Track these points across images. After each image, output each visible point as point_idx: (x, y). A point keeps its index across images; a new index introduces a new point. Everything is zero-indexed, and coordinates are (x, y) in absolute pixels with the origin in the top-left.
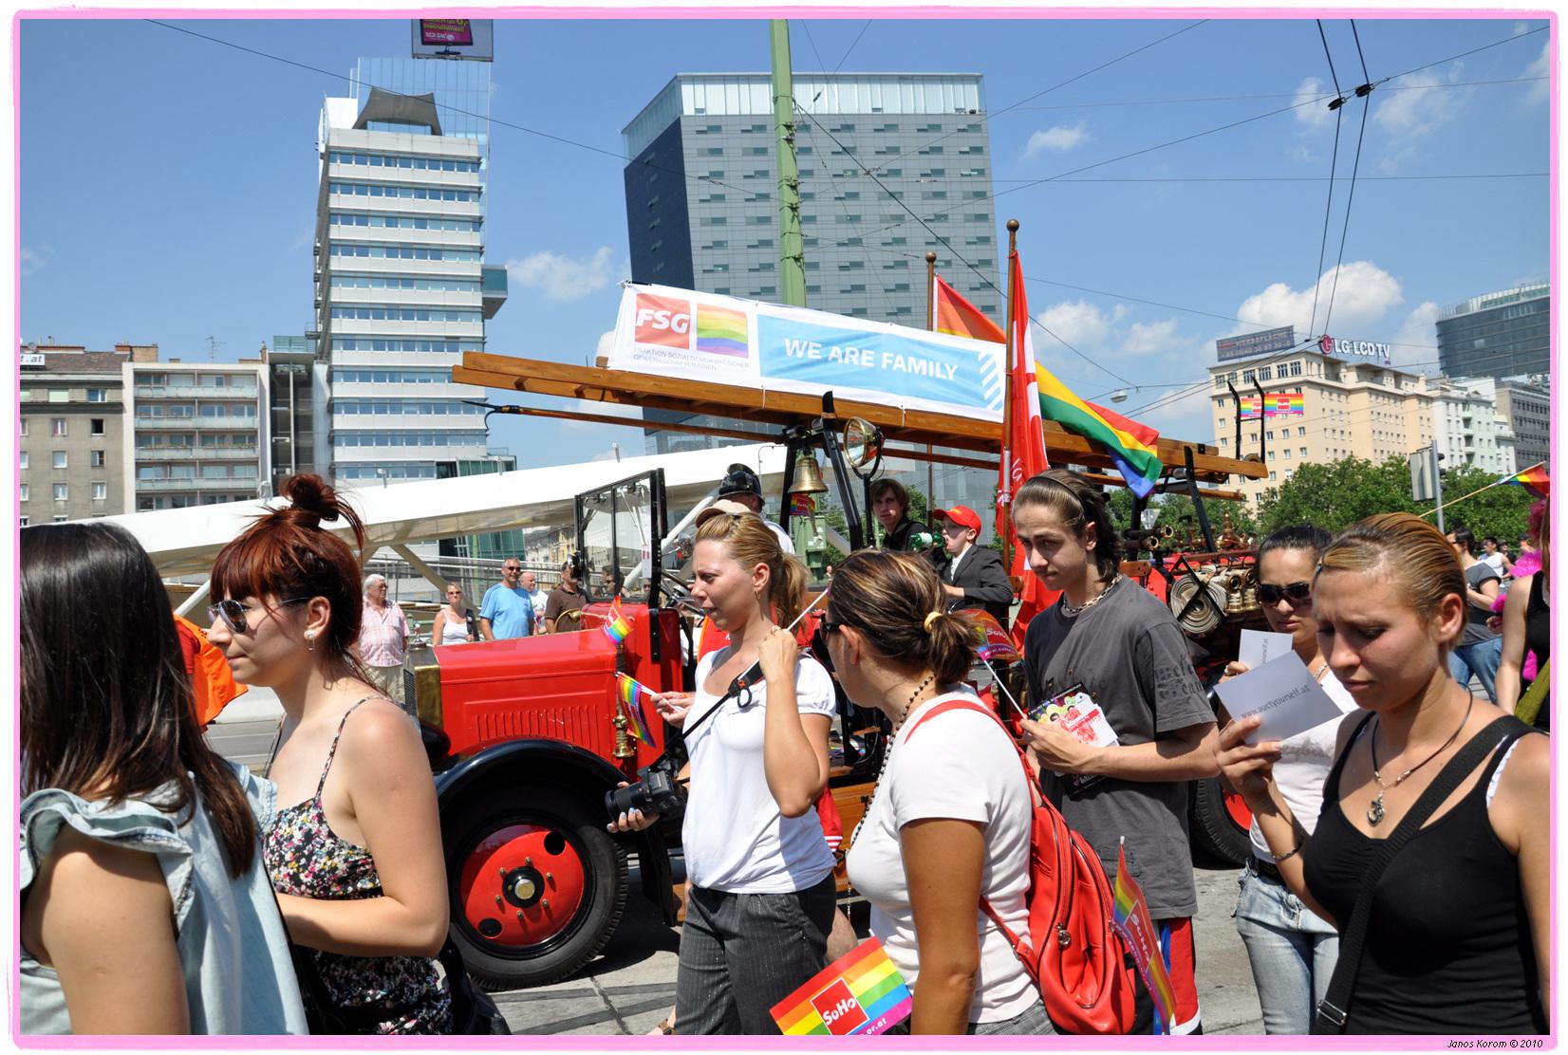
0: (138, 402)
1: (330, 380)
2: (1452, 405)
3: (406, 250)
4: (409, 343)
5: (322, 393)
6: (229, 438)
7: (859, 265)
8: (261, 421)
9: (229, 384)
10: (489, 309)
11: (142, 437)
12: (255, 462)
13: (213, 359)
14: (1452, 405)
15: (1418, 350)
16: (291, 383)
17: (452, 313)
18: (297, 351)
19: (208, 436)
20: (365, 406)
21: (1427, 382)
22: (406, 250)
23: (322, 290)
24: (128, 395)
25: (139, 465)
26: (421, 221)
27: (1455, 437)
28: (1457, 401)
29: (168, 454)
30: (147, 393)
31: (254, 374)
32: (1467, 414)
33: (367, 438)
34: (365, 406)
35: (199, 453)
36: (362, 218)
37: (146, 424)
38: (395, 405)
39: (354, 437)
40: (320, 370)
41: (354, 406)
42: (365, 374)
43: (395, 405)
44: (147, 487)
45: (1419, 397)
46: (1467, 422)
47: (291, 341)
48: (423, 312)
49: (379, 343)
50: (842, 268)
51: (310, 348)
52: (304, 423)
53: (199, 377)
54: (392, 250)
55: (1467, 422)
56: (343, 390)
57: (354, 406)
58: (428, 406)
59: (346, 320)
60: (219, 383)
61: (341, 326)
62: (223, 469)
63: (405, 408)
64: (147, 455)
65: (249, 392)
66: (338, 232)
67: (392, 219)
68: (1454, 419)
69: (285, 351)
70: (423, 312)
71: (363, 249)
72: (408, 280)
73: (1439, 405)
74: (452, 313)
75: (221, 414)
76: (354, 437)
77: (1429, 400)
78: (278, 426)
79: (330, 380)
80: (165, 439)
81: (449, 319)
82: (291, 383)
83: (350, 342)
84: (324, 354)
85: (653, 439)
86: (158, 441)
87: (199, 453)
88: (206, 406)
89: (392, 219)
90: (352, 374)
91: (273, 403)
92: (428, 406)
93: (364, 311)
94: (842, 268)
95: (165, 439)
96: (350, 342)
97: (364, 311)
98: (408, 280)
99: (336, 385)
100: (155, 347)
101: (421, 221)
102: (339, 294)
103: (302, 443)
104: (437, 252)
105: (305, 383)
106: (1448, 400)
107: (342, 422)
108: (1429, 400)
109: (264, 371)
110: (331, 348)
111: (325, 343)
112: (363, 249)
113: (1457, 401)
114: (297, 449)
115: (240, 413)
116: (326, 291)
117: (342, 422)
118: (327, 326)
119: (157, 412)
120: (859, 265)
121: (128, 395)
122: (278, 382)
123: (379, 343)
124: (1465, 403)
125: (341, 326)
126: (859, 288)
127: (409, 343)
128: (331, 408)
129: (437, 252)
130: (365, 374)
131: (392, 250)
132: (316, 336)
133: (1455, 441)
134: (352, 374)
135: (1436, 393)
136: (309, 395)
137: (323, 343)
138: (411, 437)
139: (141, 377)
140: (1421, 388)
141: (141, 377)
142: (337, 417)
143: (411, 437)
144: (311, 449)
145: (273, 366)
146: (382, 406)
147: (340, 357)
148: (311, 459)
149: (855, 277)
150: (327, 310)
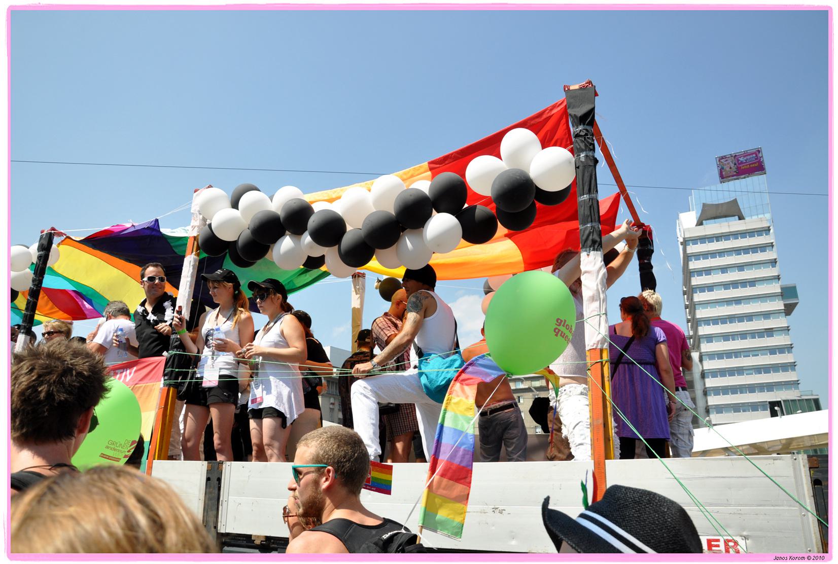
1: (701, 360)
3: (735, 284)
4: (743, 335)
5: (697, 369)
17: (767, 315)
20: (722, 372)
22: (735, 284)
23: (690, 313)
26: (741, 267)
33: (725, 390)
34: (722, 372)
36: (708, 271)
38: (740, 371)
39: (718, 391)
41: (716, 373)
42: (720, 355)
43: (740, 371)
48: (749, 317)
49: (726, 337)
54: (726, 286)
56: (708, 365)
57: (716, 373)
58: (759, 370)
59: (707, 327)
63: (745, 372)
66: (696, 281)
67: (724, 269)
70: (749, 317)
71: (710, 288)
72: (738, 301)
74: (767, 315)
76: (718, 391)
79: (701, 360)
81: (765, 319)
83: (710, 338)
89: (724, 269)
90: (713, 356)
92: (759, 370)
93: (715, 321)
96: (710, 338)
97: (715, 321)
98: (738, 301)
99: (705, 362)
101: (741, 267)
104: (752, 283)
107: (710, 382)
110: (699, 343)
112: (710, 288)
117: (710, 382)
118: (696, 331)
123: (726, 337)
127: (743, 335)
128: (703, 375)
129: (752, 283)
130: (720, 355)
131: (726, 286)
134: (713, 356)
137: (694, 341)
138: (751, 388)
142: (707, 380)
143: (751, 388)
146: (732, 372)
147: (705, 347)
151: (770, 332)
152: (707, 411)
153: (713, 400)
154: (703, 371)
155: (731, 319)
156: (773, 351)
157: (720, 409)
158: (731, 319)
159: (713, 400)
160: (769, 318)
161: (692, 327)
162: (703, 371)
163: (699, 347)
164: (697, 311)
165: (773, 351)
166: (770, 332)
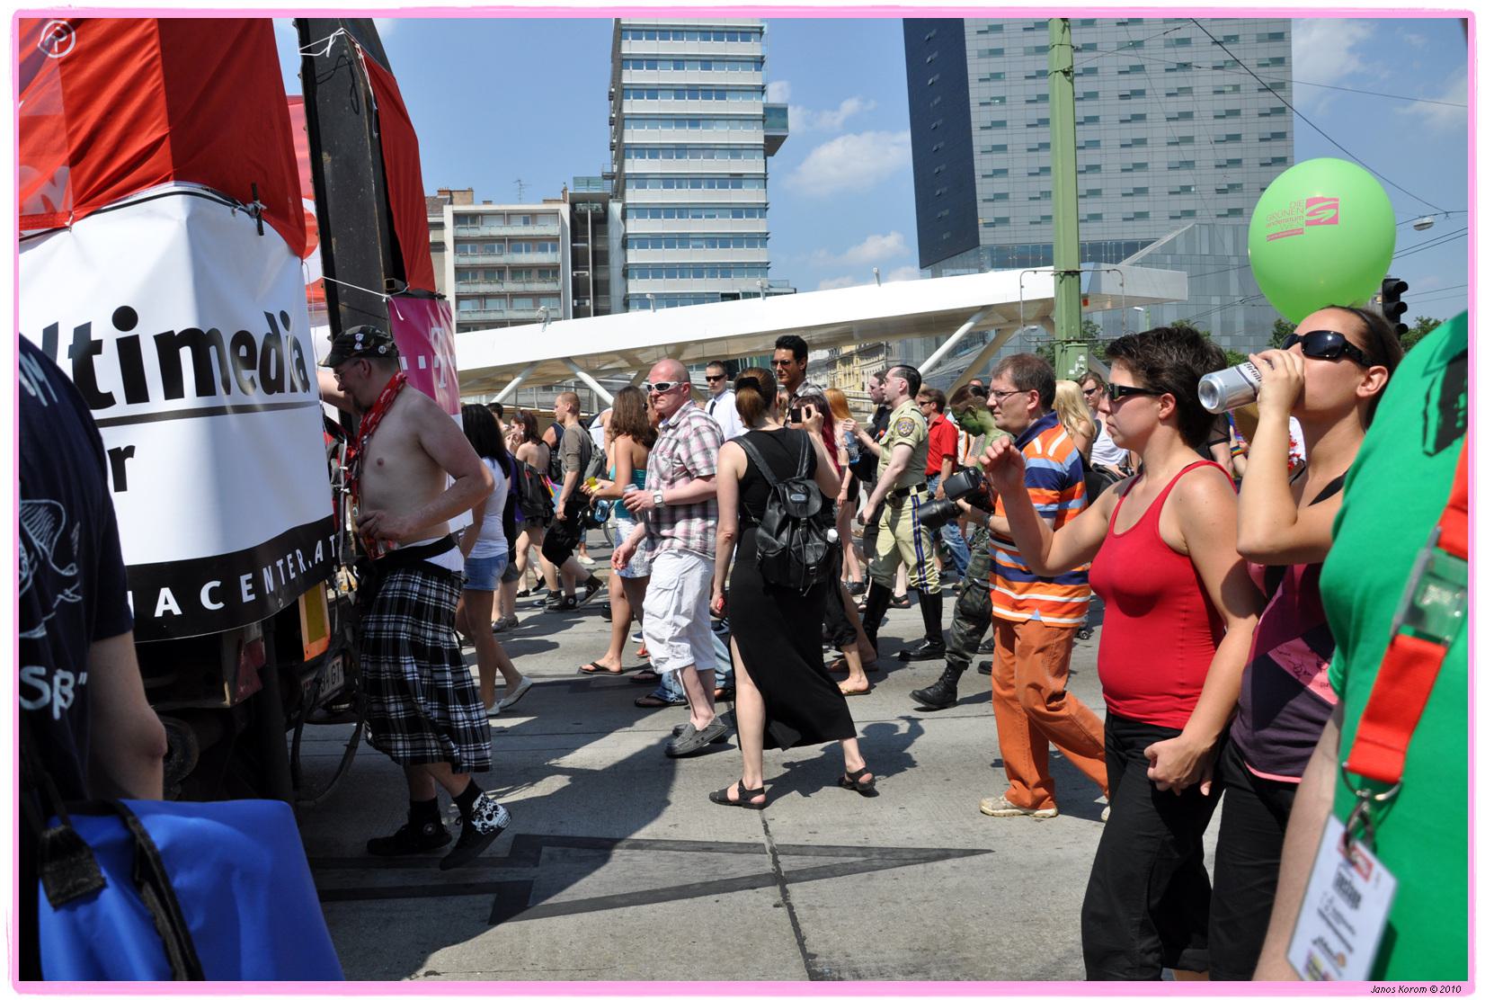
0: (457, 241)
1: (624, 217)
3: (693, 91)
4: (695, 181)
6: (535, 273)
7: (1141, 93)
8: (560, 257)
9: (535, 222)
10: (772, 145)
11: (461, 273)
12: (557, 295)
13: (520, 201)
16: (589, 222)
17: (735, 151)
18: (594, 190)
19: (517, 271)
20: (656, 241)
22: (693, 91)
23: (616, 132)
24: (448, 235)
25: (459, 298)
29: (483, 288)
30: (466, 232)
31: (556, 213)
34: (656, 241)
35: (510, 286)
37: (465, 261)
38: (683, 240)
39: (646, 271)
40: (615, 208)
42: (656, 211)
43: (683, 240)
44: (466, 317)
47: (589, 181)
49: (668, 181)
50: (1123, 97)
51: (607, 187)
52: (601, 258)
53: (508, 217)
54: (679, 92)
56: (635, 226)
58: (713, 240)
60: (526, 222)
61: (634, 166)
62: (530, 301)
63: (692, 243)
64: (465, 289)
65: (552, 229)
69: (583, 190)
71: (653, 92)
72: (694, 121)
74: (735, 151)
75: (528, 251)
76: (646, 271)
78: (578, 261)
79: (624, 217)
80: (480, 275)
82: (589, 222)
83: (642, 180)
84: (619, 193)
85: (928, 272)
86: (475, 277)
87: (510, 286)
88: (514, 243)
91: (573, 240)
92: (713, 240)
93: (653, 151)
94: (1123, 97)
95: (480, 275)
96: (642, 180)
97: (653, 151)
98: (694, 121)
99: (630, 222)
100: (471, 190)
102: (632, 136)
103: (601, 276)
104: (721, 92)
105: (602, 220)
107: (635, 256)
109: (565, 210)
111: (620, 182)
112: (653, 92)
114: (595, 282)
115: (544, 249)
116: (619, 133)
117: (635, 256)
118: (621, 167)
119: (473, 250)
120: (1141, 93)
121: (448, 235)
122: (577, 220)
123: (668, 181)
125: (634, 166)
126: (1140, 117)
127: (695, 181)
128: (625, 243)
129: (721, 92)
130: (656, 211)
131: (679, 92)
132: (612, 177)
136: (606, 232)
138: (698, 270)
139: (459, 218)
141: (459, 218)
142: (630, 252)
143: (698, 270)
144: (607, 282)
145: (573, 206)
147: (634, 196)
148: (607, 291)
149: (1136, 106)
150: (621, 151)
151: (737, 180)
152: (626, 305)
153: (636, 286)
154: (625, 235)
155: (680, 150)
156: (738, 211)
157: (644, 302)
158: (680, 150)
159: (636, 286)
160: (738, 156)
161: (616, 158)
162: (625, 235)
163: (623, 194)
164: (627, 132)
165: (738, 211)
166: (737, 180)
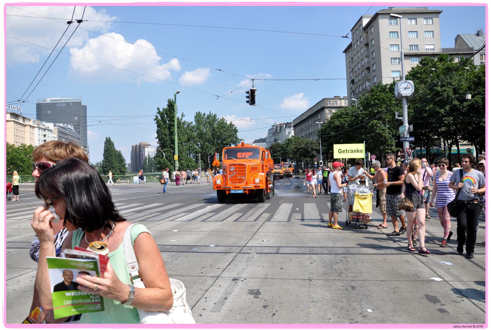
2: (41, 130)
14: (41, 130)
15: (30, 111)
21: (33, 122)
27: (41, 140)
28: (42, 129)
32: (45, 133)
45: (31, 126)
46: (45, 135)
55: (45, 135)
68: (41, 134)
73: (36, 129)
77: (34, 127)
106: (39, 128)
108: (34, 127)
113: (42, 129)
124: (45, 130)
133: (41, 141)
135: (36, 126)
140: (31, 123)
